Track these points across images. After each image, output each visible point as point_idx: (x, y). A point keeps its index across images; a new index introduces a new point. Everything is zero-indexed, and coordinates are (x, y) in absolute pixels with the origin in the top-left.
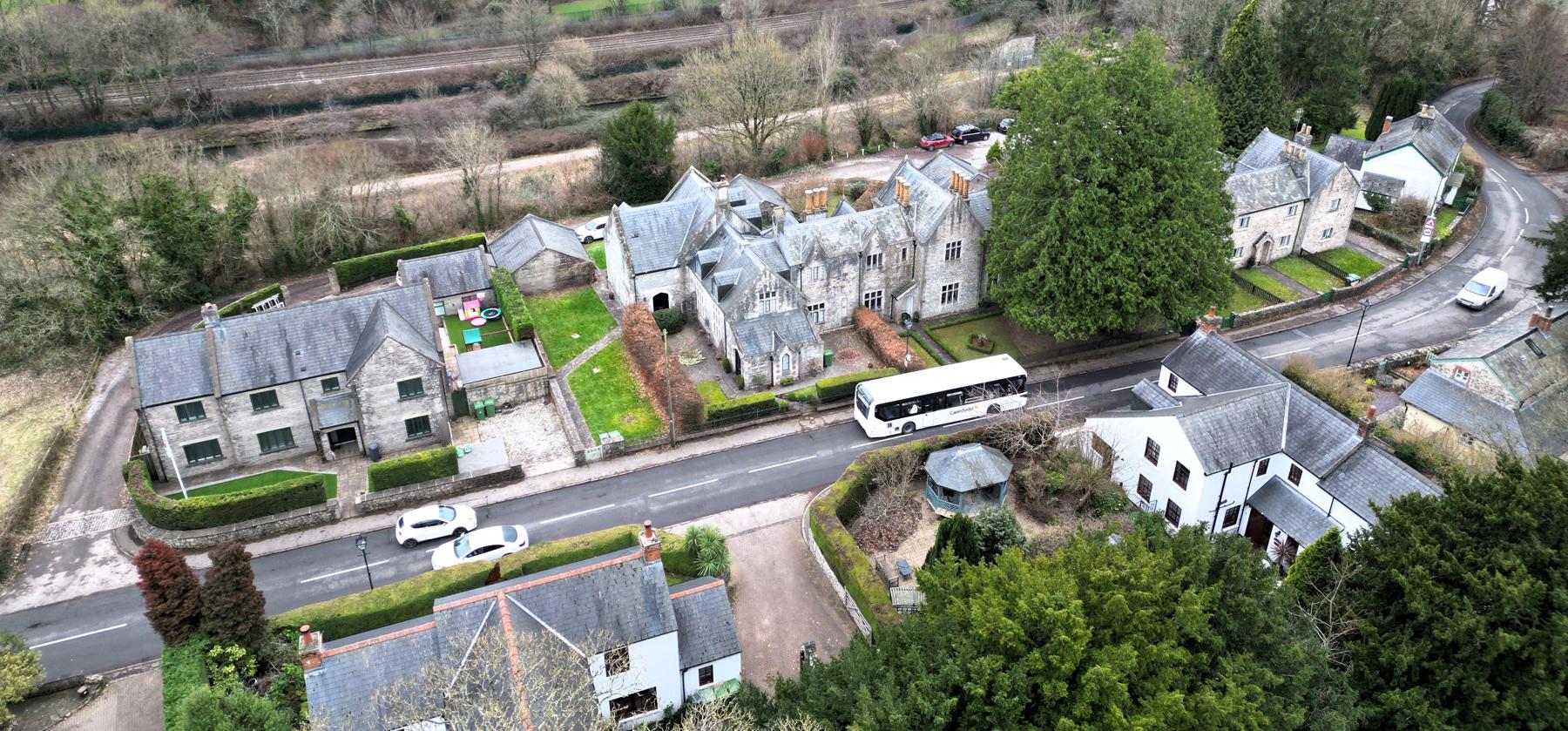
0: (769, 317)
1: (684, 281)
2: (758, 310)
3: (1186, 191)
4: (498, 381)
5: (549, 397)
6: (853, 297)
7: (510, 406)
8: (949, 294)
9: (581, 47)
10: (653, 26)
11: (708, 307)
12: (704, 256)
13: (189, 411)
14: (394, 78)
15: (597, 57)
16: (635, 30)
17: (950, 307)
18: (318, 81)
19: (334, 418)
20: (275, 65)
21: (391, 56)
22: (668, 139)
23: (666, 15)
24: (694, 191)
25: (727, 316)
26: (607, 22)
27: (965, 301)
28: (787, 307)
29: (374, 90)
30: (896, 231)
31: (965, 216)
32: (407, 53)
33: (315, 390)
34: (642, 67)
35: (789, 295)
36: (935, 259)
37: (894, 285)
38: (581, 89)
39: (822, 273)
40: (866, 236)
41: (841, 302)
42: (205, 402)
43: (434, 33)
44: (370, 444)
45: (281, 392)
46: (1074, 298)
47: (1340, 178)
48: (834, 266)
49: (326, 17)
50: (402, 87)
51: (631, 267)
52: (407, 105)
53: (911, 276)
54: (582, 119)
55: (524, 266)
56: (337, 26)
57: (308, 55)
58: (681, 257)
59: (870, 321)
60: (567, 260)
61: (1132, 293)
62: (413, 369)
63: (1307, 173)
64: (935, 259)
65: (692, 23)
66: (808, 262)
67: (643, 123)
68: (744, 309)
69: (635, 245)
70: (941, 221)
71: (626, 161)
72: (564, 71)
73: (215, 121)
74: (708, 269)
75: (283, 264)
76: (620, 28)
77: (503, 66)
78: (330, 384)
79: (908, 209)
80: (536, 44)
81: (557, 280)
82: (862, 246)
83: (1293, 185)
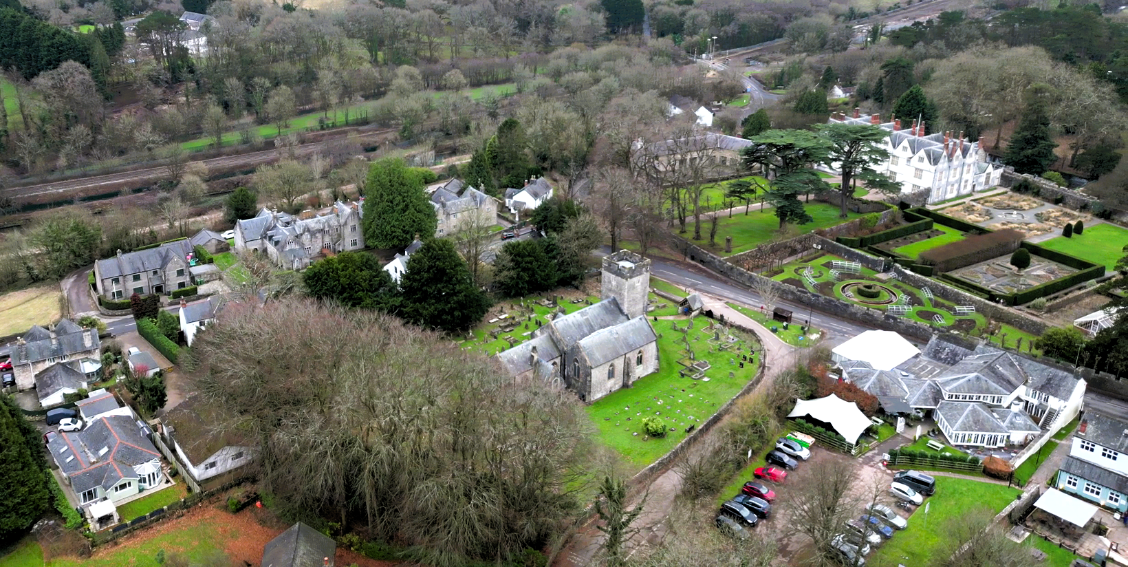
0: (291, 250)
1: (263, 244)
2: (288, 248)
3: (411, 202)
4: (204, 273)
5: (220, 279)
6: (321, 244)
7: (208, 282)
8: (354, 243)
9: (201, 165)
10: (237, 153)
11: (271, 248)
12: (269, 233)
13: (116, 280)
14: (101, 187)
15: (210, 170)
16: (228, 155)
17: (354, 248)
18: (61, 191)
19: (157, 283)
20: (33, 184)
21: (94, 176)
22: (253, 201)
23: (244, 146)
24: (266, 214)
25: (278, 250)
26: (212, 152)
27: (360, 245)
28: (297, 247)
29: (92, 194)
30: (334, 222)
31: (356, 216)
32: (102, 174)
33: (151, 274)
34: (234, 175)
35: (298, 243)
36: (347, 231)
37: (335, 241)
38: (204, 186)
39: (309, 236)
40: (324, 224)
41: (317, 246)
42: (121, 279)
43: (116, 161)
44: (167, 290)
45: (143, 276)
46: (386, 237)
47: (487, 200)
48: (313, 233)
49: (57, 158)
50: (114, 191)
51: (244, 239)
52: (119, 198)
53: (340, 236)
54: (206, 201)
55: (205, 245)
56: (62, 161)
57: (50, 177)
58: (261, 235)
59: (325, 251)
60: (220, 242)
61: (399, 232)
62: (181, 266)
63: (478, 200)
64: (347, 231)
65: (259, 150)
66: (304, 233)
67: (244, 195)
68: (283, 247)
69: (245, 232)
70: (348, 218)
71: (237, 210)
72: (196, 179)
73: (14, 212)
74: (271, 238)
75: (110, 252)
76: (219, 155)
77: (159, 179)
78: (155, 273)
79: (338, 215)
80: (177, 164)
81: (217, 249)
82: (322, 227)
83: (473, 203)
